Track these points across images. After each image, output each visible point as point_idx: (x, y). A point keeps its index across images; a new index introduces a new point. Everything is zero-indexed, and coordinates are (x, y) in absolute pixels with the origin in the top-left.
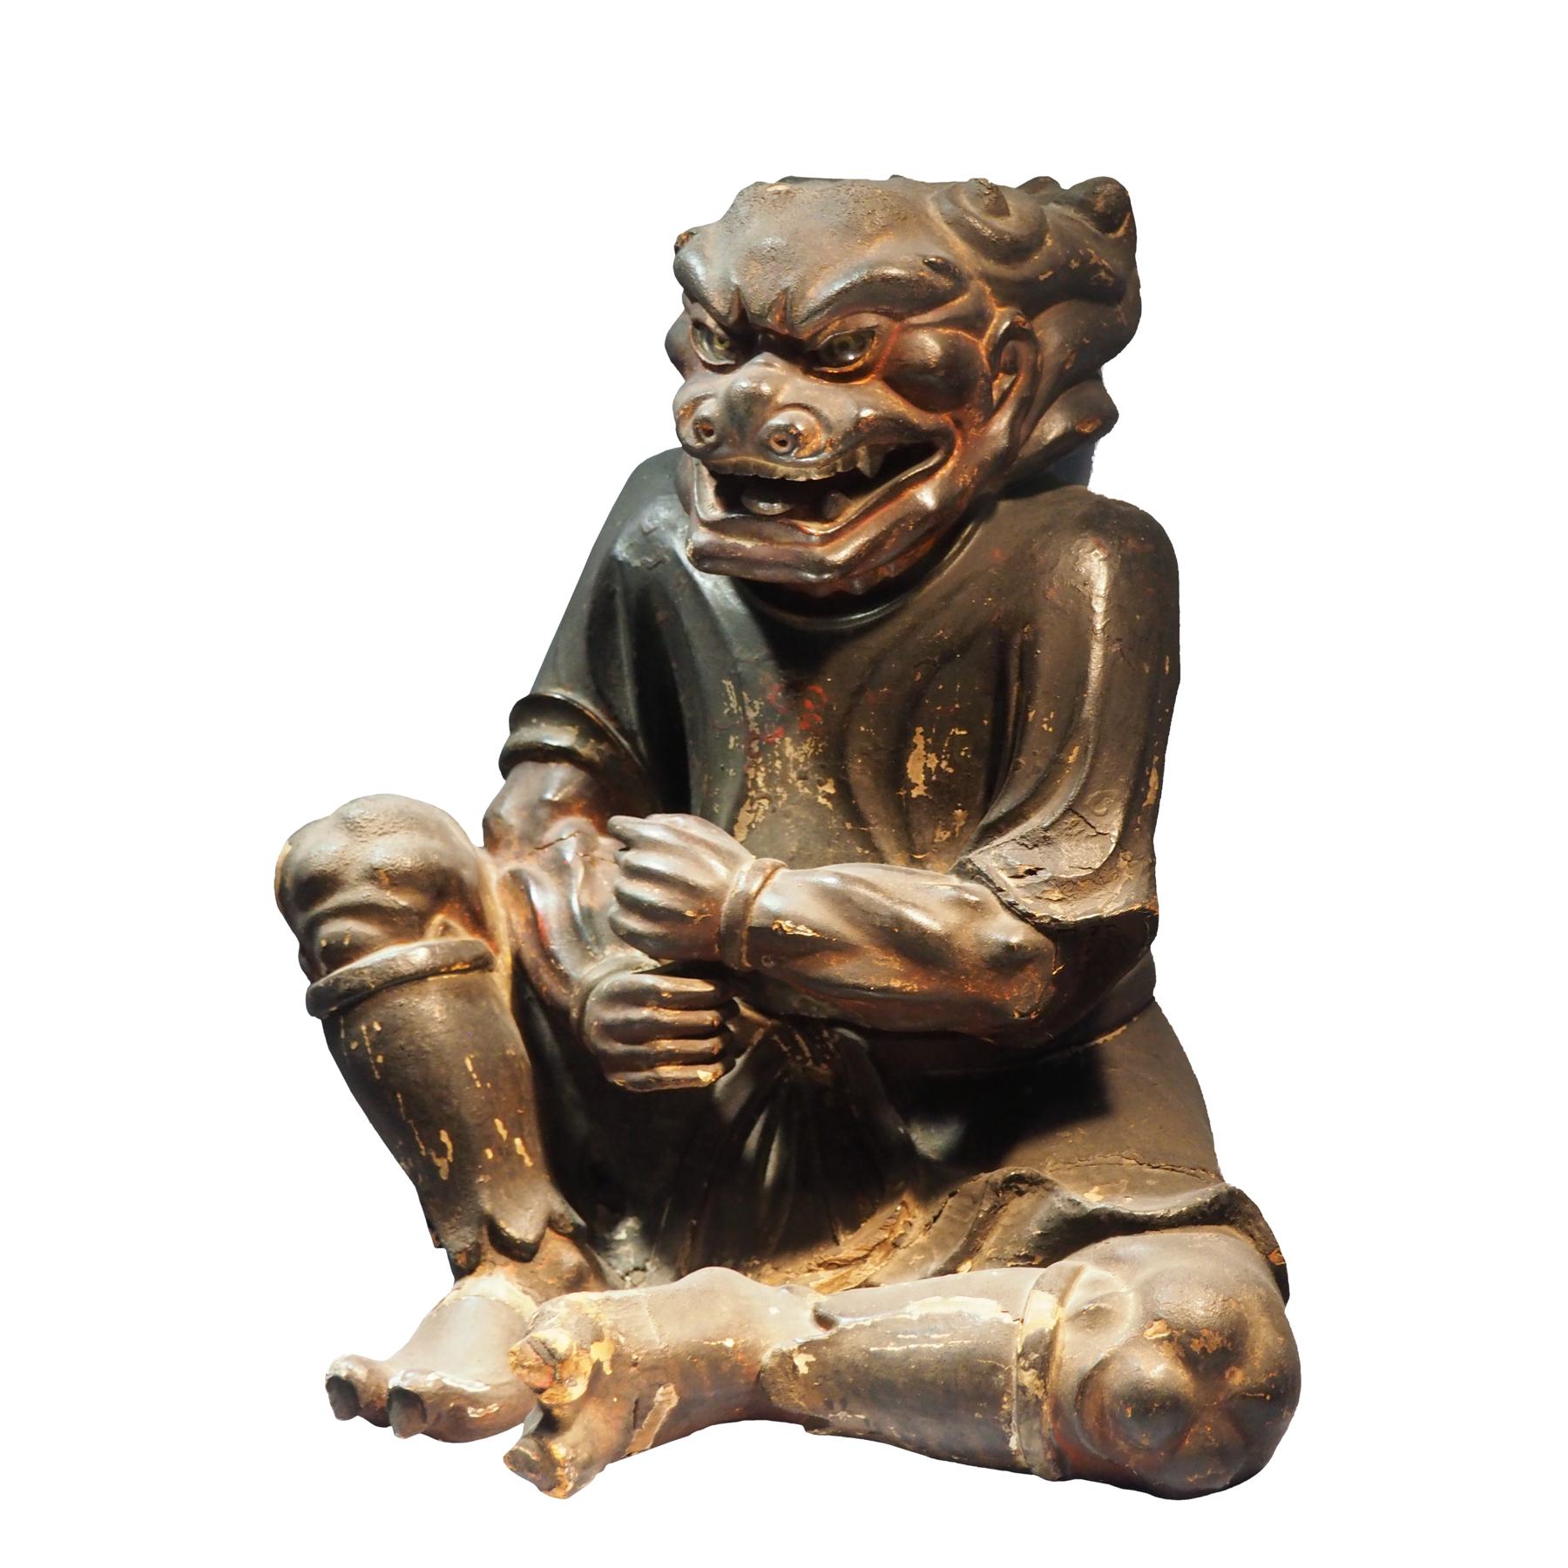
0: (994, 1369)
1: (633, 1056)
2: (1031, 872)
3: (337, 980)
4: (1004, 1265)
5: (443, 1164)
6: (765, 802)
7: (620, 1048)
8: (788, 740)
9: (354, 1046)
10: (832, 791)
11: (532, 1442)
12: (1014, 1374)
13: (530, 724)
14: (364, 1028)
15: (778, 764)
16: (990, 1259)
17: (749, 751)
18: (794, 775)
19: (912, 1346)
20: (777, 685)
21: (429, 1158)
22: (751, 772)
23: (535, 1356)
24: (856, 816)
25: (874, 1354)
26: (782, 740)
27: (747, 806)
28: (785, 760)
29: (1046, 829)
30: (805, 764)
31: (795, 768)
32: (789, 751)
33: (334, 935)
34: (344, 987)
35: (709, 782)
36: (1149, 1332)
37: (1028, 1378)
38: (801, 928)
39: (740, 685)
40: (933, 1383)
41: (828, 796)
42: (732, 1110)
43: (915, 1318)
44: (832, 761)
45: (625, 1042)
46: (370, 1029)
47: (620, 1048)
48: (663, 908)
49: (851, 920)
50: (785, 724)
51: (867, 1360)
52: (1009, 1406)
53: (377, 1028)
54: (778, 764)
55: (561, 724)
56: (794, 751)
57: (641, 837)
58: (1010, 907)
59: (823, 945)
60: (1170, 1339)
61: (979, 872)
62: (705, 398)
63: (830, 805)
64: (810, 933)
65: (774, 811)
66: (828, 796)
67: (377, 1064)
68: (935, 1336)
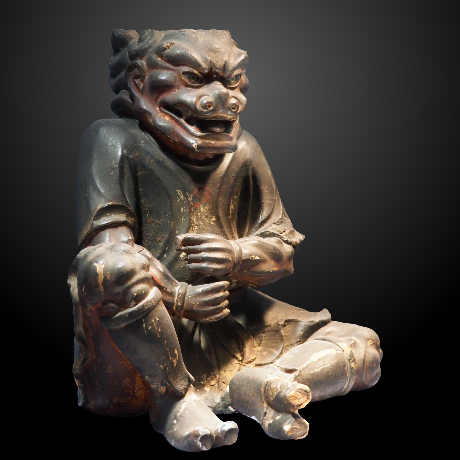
0: (344, 365)
1: (217, 309)
2: (284, 231)
3: (143, 306)
4: (294, 346)
5: (175, 361)
6: (196, 227)
7: (211, 308)
8: (201, 206)
9: (150, 328)
10: (215, 220)
11: (296, 423)
12: (349, 365)
13: (106, 216)
14: (153, 320)
15: (199, 214)
16: (288, 346)
17: (191, 211)
18: (204, 217)
19: (322, 368)
20: (196, 190)
21: (172, 360)
22: (192, 218)
23: (300, 394)
24: (221, 226)
25: (313, 374)
26: (200, 206)
27: (191, 229)
28: (200, 212)
29: (281, 219)
30: (207, 213)
31: (204, 214)
32: (202, 209)
33: (139, 290)
34: (146, 308)
35: (174, 224)
36: (368, 343)
37: (353, 365)
38: (257, 257)
39: (185, 191)
40: (332, 375)
41: (214, 222)
42: (190, 329)
43: (316, 360)
44: (214, 211)
45: (213, 305)
46: (155, 320)
47: (211, 308)
48: (225, 259)
49: (264, 252)
50: (199, 200)
51: (311, 376)
52: (348, 375)
53: (158, 319)
54: (199, 214)
55: (119, 214)
56: (203, 209)
57: (208, 239)
58: (286, 242)
59: (262, 261)
60: (373, 344)
61: (274, 233)
62: (203, 96)
63: (214, 224)
64: (258, 258)
65: (199, 229)
66: (214, 222)
67: (159, 332)
68: (326, 363)
